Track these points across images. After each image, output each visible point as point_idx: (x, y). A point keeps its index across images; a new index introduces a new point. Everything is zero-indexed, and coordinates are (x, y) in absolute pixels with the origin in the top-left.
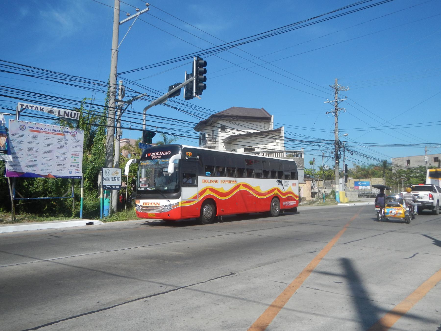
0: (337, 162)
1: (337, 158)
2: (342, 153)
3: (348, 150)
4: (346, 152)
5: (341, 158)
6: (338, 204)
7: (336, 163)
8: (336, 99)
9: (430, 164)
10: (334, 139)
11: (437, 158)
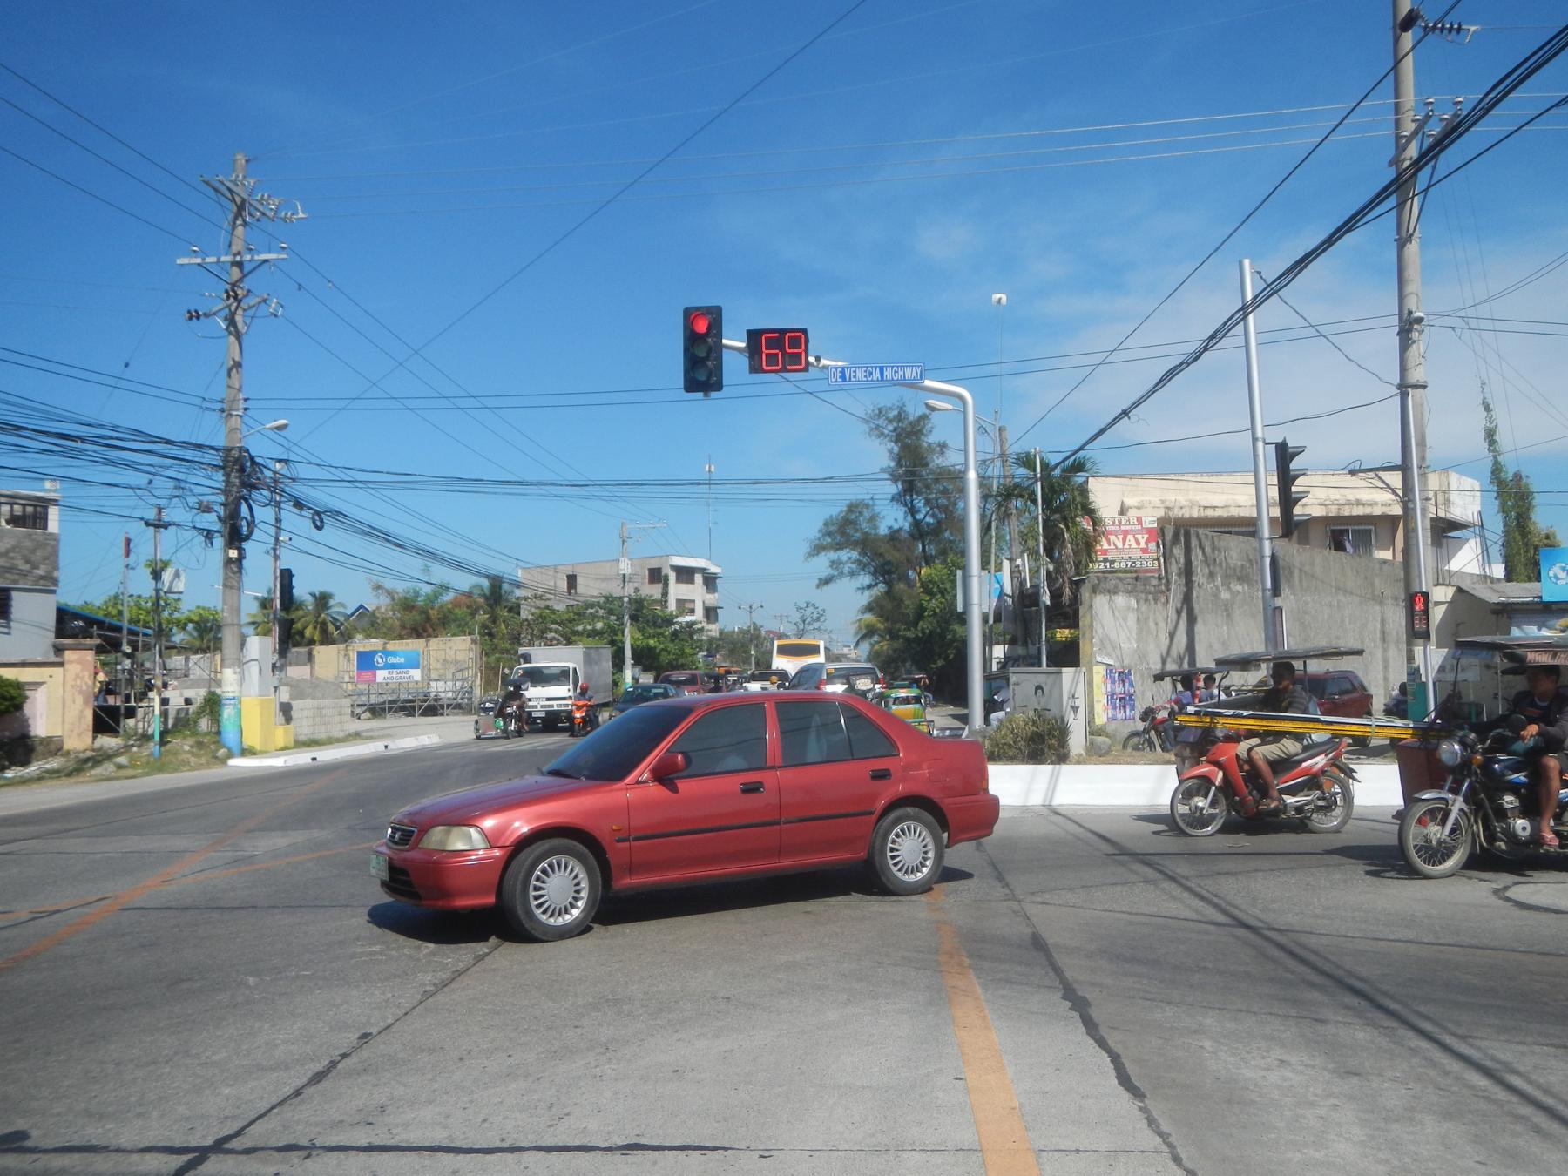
0: (233, 553)
1: (236, 537)
2: (264, 514)
3: (299, 504)
4: (290, 516)
5: (257, 534)
6: (232, 762)
7: (229, 561)
8: (235, 249)
9: (637, 590)
10: (220, 442)
11: (659, 570)
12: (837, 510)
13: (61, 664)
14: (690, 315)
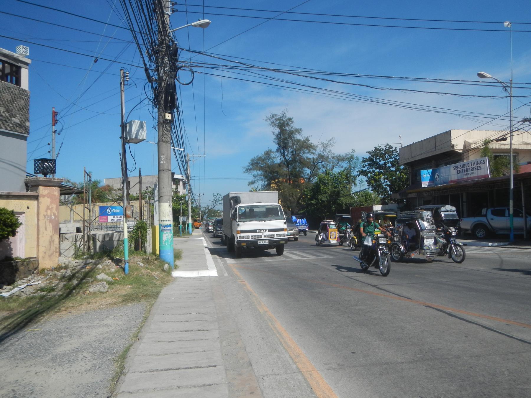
12: (261, 153)
13: (36, 198)
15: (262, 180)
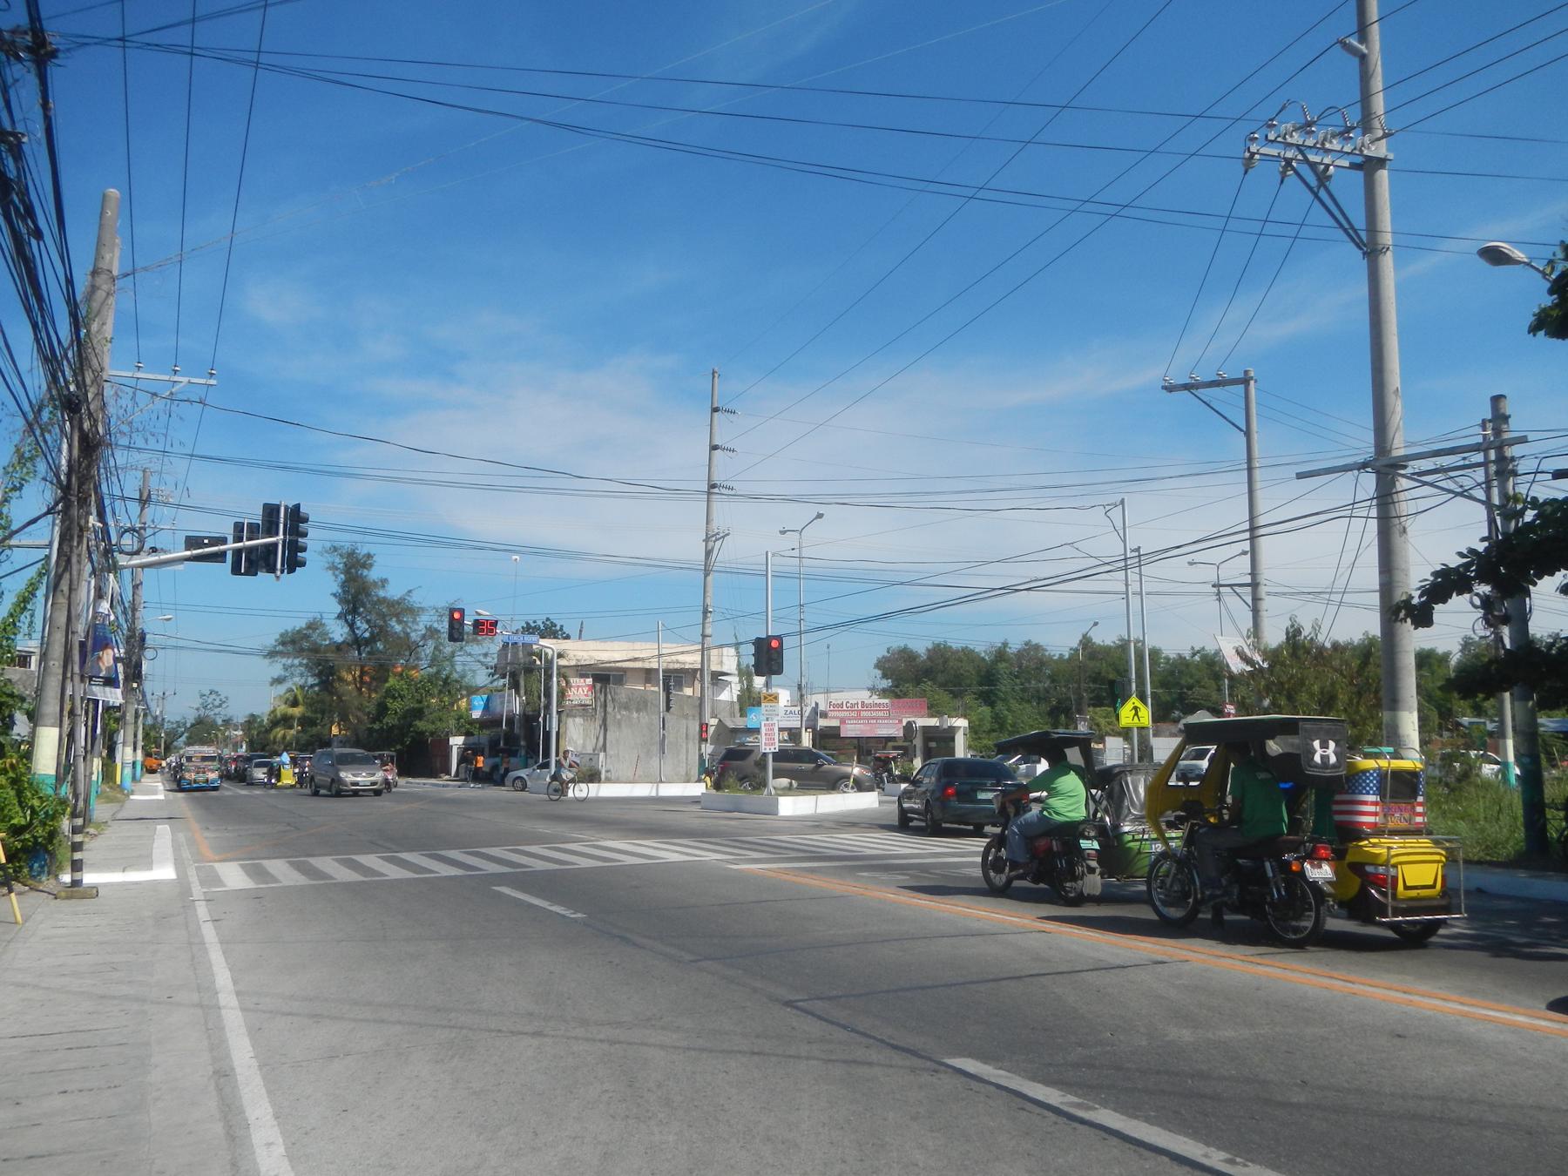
12: (300, 624)
14: (452, 611)
15: (302, 675)
